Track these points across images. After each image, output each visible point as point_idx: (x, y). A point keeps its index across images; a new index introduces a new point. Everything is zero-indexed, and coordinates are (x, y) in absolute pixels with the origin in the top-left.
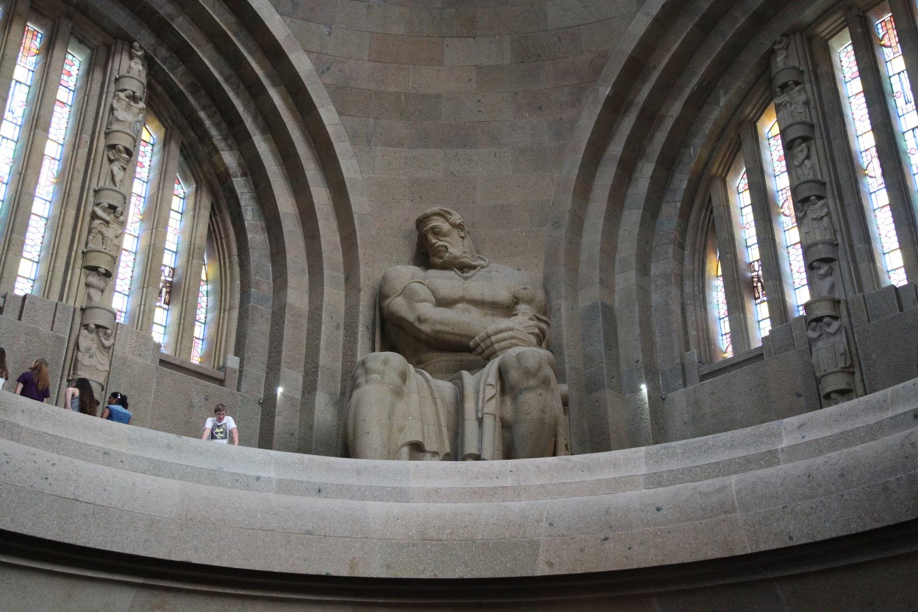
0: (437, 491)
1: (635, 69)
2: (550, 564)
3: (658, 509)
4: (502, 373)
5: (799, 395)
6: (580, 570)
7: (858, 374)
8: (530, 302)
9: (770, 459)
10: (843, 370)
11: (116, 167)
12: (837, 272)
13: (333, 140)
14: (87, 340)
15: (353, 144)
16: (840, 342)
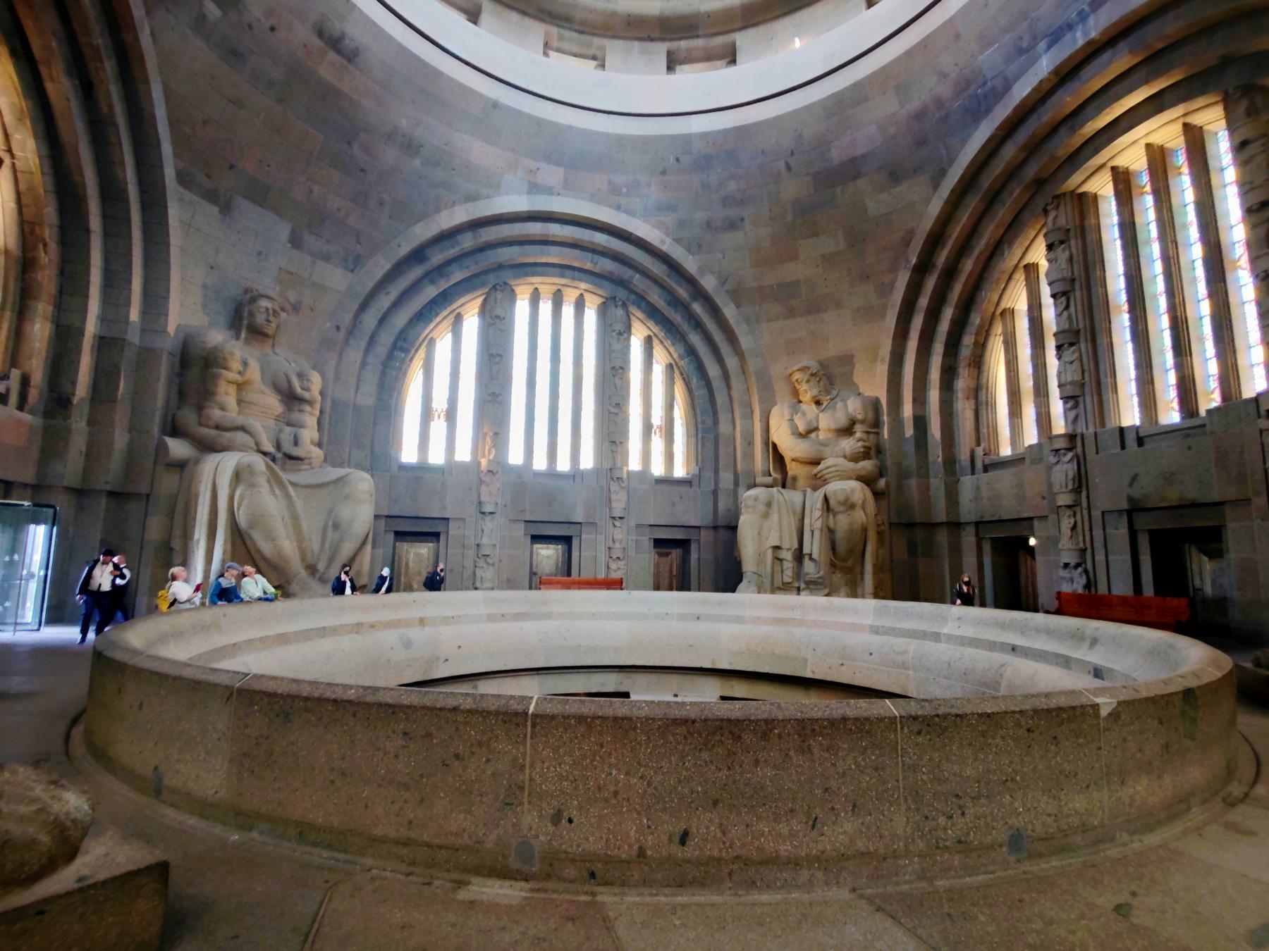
0: (759, 618)
1: (935, 240)
4: (826, 499)
5: (1044, 498)
6: (829, 679)
7: (1084, 494)
8: (862, 422)
9: (936, 637)
10: (1071, 491)
11: (617, 380)
12: (1081, 406)
13: (734, 327)
14: (614, 487)
15: (748, 325)
16: (1071, 469)
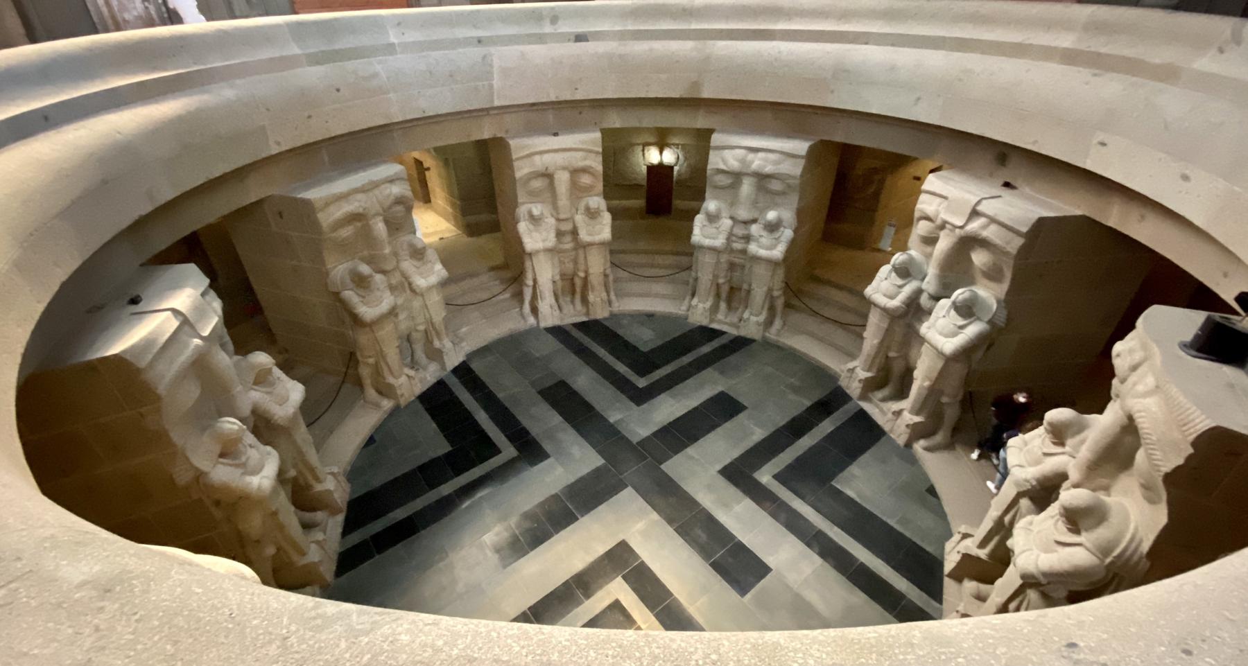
2: (278, 144)
3: (338, 90)
